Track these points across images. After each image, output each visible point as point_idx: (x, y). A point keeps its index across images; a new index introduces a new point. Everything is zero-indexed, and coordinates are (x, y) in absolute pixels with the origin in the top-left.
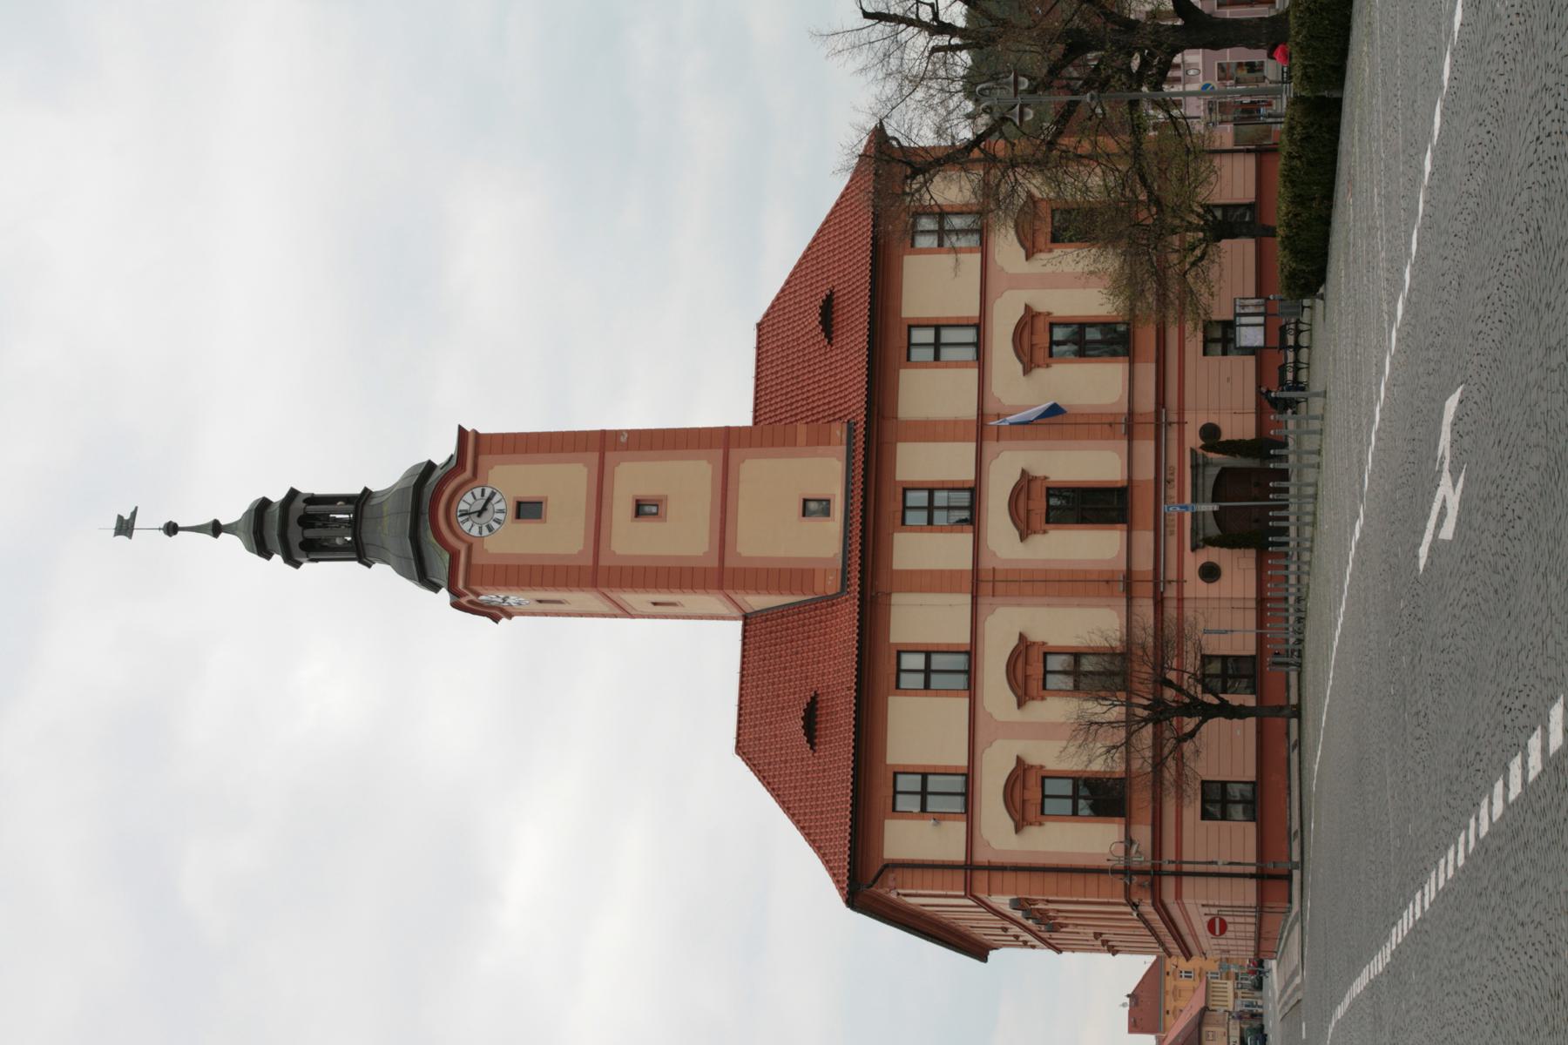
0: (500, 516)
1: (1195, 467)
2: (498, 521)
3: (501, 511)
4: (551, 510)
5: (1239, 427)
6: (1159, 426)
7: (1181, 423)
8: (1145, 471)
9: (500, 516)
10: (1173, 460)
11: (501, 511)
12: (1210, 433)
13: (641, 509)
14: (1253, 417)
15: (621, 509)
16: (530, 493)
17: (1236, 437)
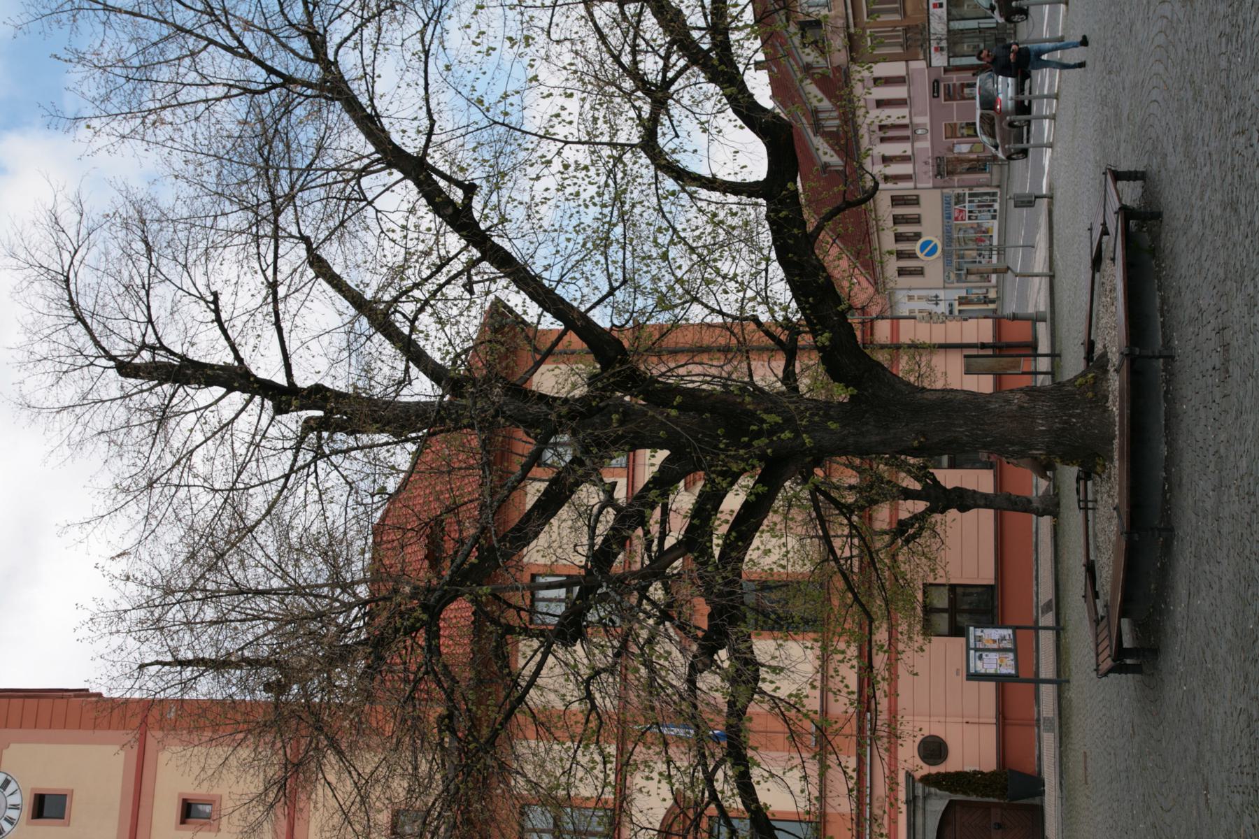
0: (14, 814)
1: (911, 802)
2: (10, 821)
3: (15, 807)
4: (76, 808)
5: (973, 750)
6: (866, 736)
7: (894, 736)
8: (841, 805)
9: (14, 814)
10: (881, 789)
11: (15, 807)
12: (933, 749)
13: (188, 811)
14: (993, 729)
15: (165, 811)
16: (50, 784)
17: (968, 768)
